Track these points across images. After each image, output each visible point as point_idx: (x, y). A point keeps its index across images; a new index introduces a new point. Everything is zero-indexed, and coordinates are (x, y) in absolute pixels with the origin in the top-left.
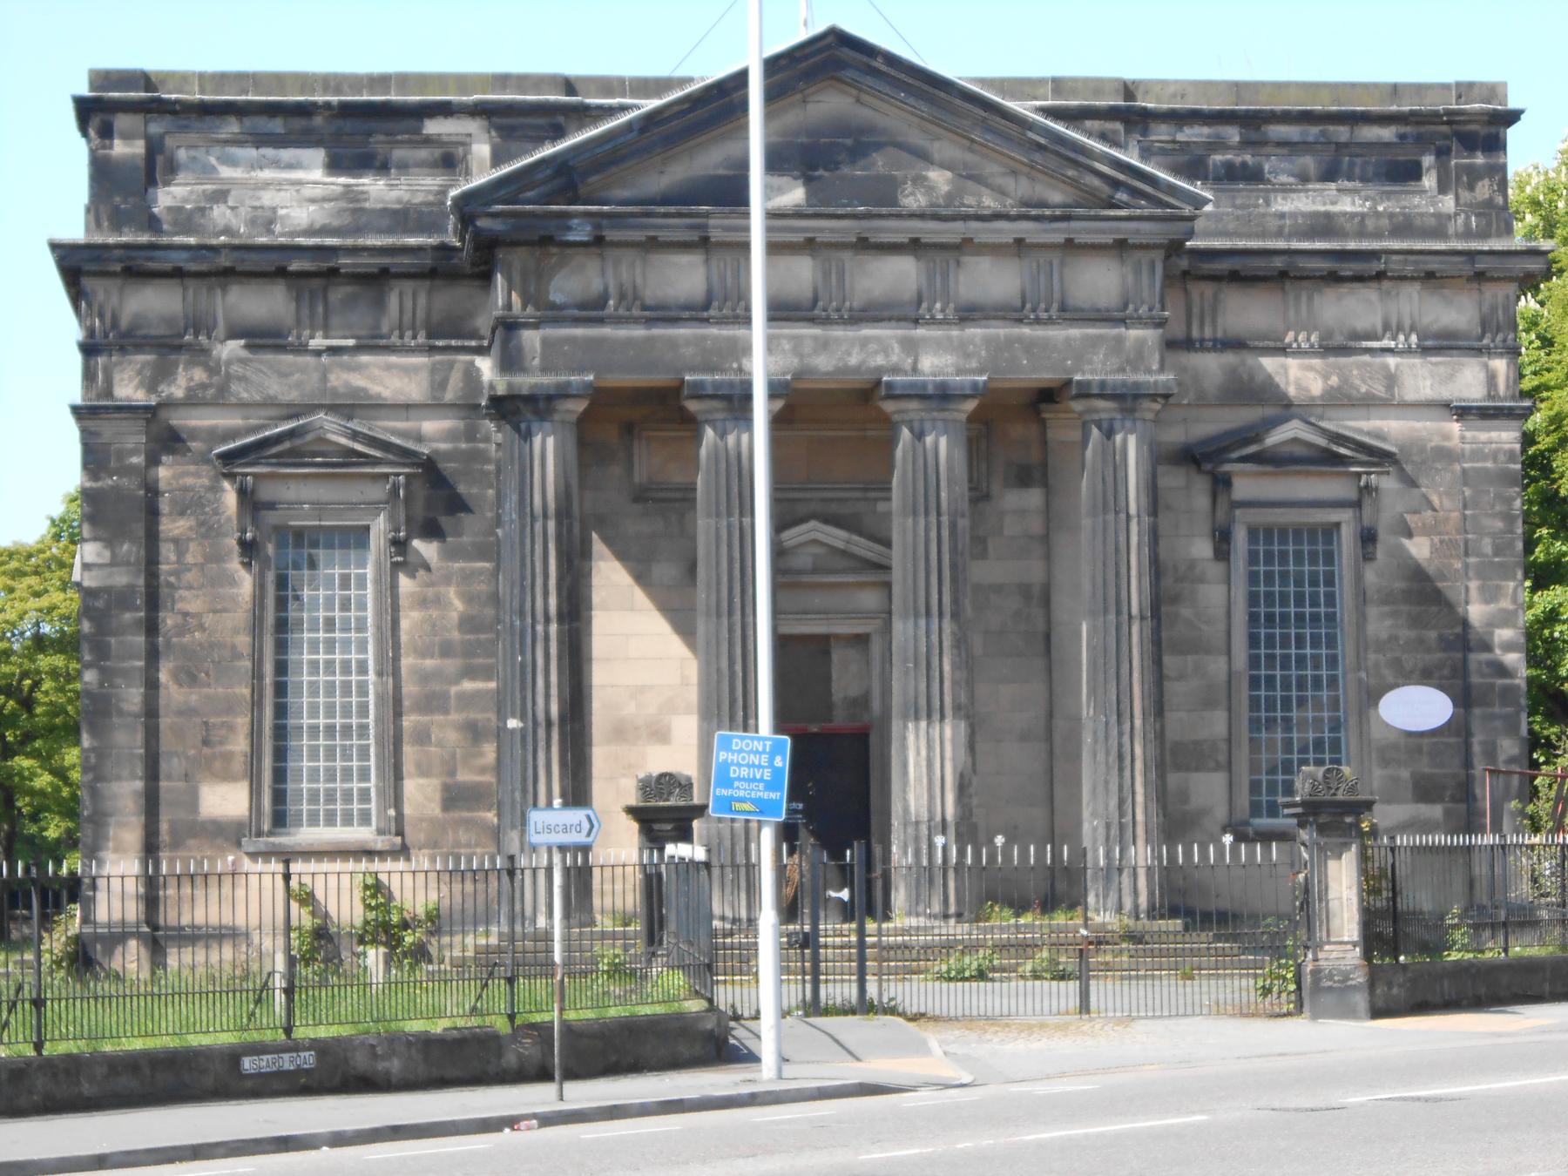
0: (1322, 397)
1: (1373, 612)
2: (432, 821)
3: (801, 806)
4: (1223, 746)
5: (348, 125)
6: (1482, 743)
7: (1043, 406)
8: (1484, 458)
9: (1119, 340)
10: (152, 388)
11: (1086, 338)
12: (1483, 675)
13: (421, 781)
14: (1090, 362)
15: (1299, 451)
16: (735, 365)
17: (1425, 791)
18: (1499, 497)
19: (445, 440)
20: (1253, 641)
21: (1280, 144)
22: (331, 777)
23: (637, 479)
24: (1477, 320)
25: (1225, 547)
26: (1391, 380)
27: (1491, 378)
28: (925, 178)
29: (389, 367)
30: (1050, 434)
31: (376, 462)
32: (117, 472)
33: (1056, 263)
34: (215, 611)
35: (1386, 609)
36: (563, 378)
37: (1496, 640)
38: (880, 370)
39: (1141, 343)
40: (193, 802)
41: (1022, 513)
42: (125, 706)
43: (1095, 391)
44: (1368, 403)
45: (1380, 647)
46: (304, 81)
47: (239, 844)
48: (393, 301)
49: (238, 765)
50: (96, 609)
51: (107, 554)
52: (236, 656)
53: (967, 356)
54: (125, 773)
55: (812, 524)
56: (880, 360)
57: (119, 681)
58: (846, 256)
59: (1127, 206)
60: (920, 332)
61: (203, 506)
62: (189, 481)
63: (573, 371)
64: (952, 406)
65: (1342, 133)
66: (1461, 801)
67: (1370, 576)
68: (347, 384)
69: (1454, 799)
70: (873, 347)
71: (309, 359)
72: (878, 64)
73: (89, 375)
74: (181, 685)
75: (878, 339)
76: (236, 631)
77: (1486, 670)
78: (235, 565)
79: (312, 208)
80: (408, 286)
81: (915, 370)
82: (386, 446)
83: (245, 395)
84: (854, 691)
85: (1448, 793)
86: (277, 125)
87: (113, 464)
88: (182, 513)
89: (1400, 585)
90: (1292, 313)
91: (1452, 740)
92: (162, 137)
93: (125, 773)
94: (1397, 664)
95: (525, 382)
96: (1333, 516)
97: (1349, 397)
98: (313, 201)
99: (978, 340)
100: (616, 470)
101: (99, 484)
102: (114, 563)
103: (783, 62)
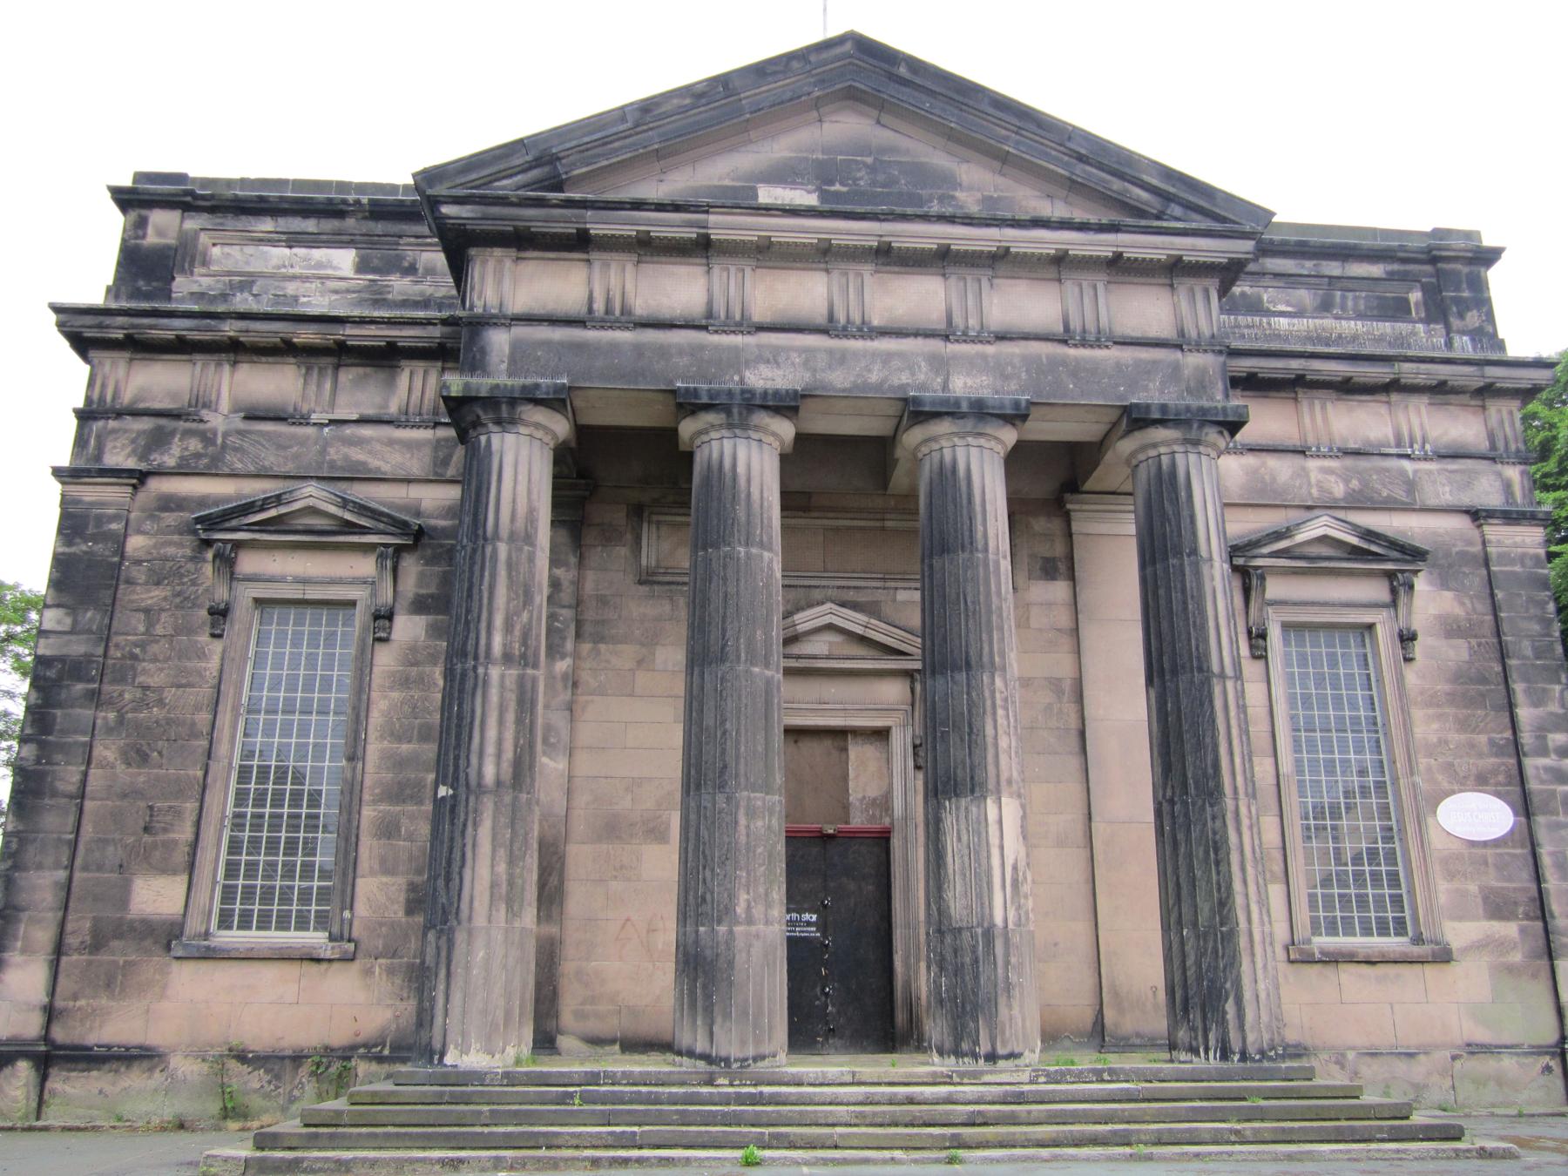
0: (1344, 499)
1: (1418, 714)
2: (393, 925)
3: (814, 917)
4: (1278, 855)
5: (379, 227)
6: (1551, 854)
7: (1068, 496)
8: (1512, 562)
9: (1176, 368)
10: (143, 457)
11: (1138, 363)
12: (1542, 782)
13: (384, 879)
14: (1146, 389)
15: (1325, 551)
16: (736, 378)
17: (1497, 908)
18: (1531, 600)
19: (444, 518)
20: (1297, 747)
21: (1277, 275)
22: (289, 872)
23: (644, 562)
24: (1484, 435)
25: (1261, 642)
26: (1411, 485)
27: (1507, 486)
28: (953, 197)
29: (391, 442)
30: (1075, 527)
31: (363, 530)
32: (95, 538)
33: (1100, 286)
34: (179, 686)
35: (1431, 711)
36: (529, 381)
37: (1550, 744)
38: (903, 387)
39: (1201, 372)
40: (123, 897)
41: (1049, 605)
42: (61, 786)
43: (1156, 415)
44: (1390, 506)
45: (1430, 751)
46: (343, 186)
47: (168, 948)
48: (403, 379)
49: (180, 856)
50: (46, 679)
51: (68, 621)
52: (194, 734)
53: (1006, 378)
54: (49, 861)
55: (829, 606)
56: (905, 378)
57: (58, 757)
58: (867, 269)
59: (1177, 219)
60: (953, 348)
61: (182, 576)
62: (171, 551)
63: (542, 376)
64: (989, 430)
65: (1333, 268)
66: (1537, 918)
67: (1411, 675)
68: (346, 458)
69: (1527, 917)
70: (896, 363)
71: (310, 430)
72: (903, 71)
73: (80, 441)
74: (129, 765)
75: (900, 355)
76: (197, 708)
77: (1544, 777)
78: (204, 638)
79: (335, 297)
80: (419, 366)
81: (945, 387)
82: (374, 514)
83: (240, 466)
84: (873, 791)
85: (1521, 910)
86: (310, 225)
87: (91, 530)
88: (158, 583)
89: (1447, 687)
90: (1307, 420)
91: (1518, 851)
92: (196, 233)
93: (49, 861)
94: (1449, 768)
95: (482, 384)
96: (1366, 617)
97: (1371, 499)
98: (336, 292)
99: (1016, 361)
100: (623, 551)
101: (73, 550)
102: (72, 631)
103: (795, 64)
